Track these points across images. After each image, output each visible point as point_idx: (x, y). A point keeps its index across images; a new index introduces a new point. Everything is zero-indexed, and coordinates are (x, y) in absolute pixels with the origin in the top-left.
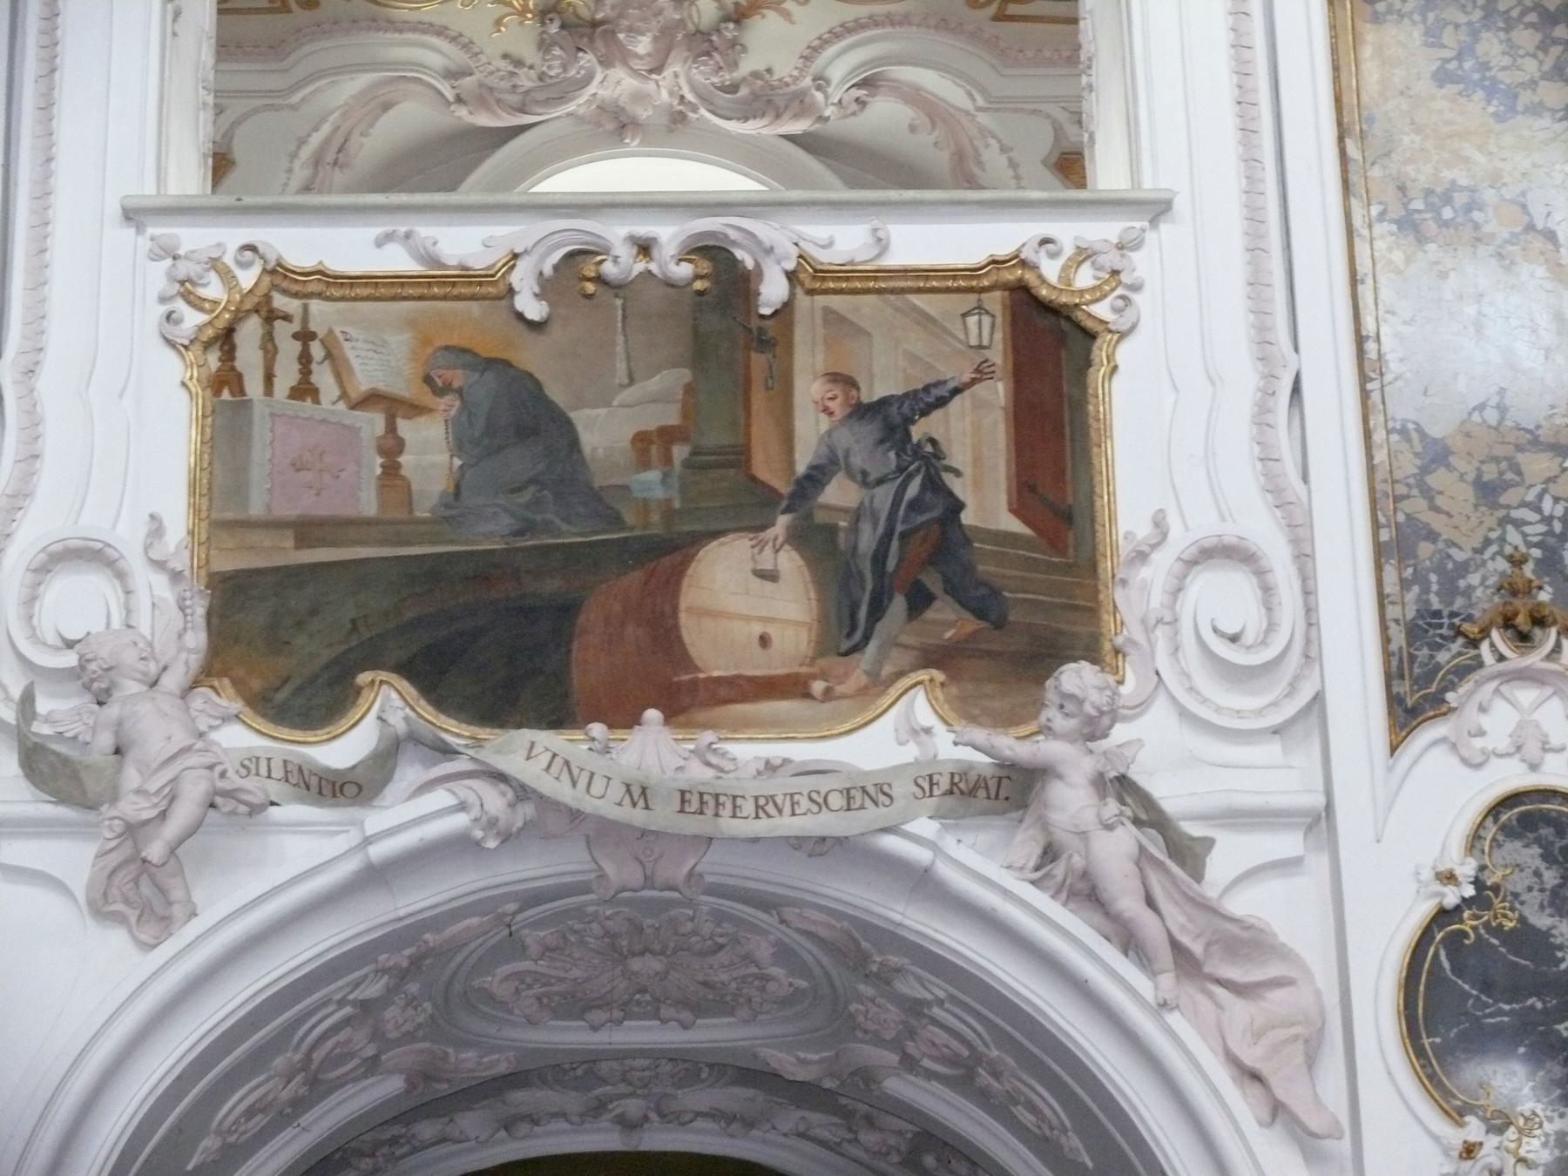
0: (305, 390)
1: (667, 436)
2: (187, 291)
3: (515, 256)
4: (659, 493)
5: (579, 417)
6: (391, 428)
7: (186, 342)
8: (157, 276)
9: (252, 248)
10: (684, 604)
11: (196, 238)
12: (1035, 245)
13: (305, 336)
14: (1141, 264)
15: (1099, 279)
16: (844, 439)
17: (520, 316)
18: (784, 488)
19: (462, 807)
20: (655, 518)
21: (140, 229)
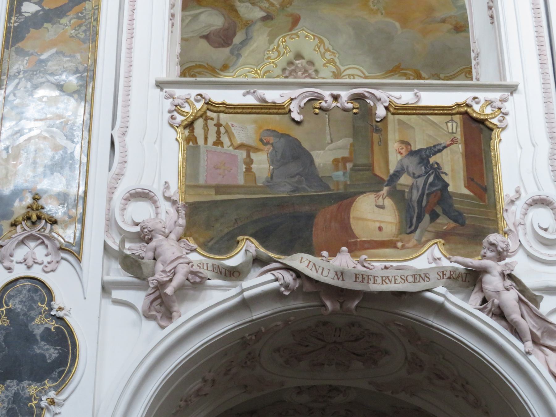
0: (218, 142)
1: (345, 160)
2: (178, 108)
3: (292, 99)
4: (342, 179)
5: (314, 154)
6: (248, 155)
7: (178, 125)
8: (168, 104)
9: (200, 95)
10: (351, 216)
11: (180, 93)
12: (472, 99)
13: (218, 125)
14: (507, 107)
15: (493, 111)
16: (406, 162)
17: (293, 120)
18: (386, 178)
19: (277, 280)
20: (341, 187)
21: (162, 89)
